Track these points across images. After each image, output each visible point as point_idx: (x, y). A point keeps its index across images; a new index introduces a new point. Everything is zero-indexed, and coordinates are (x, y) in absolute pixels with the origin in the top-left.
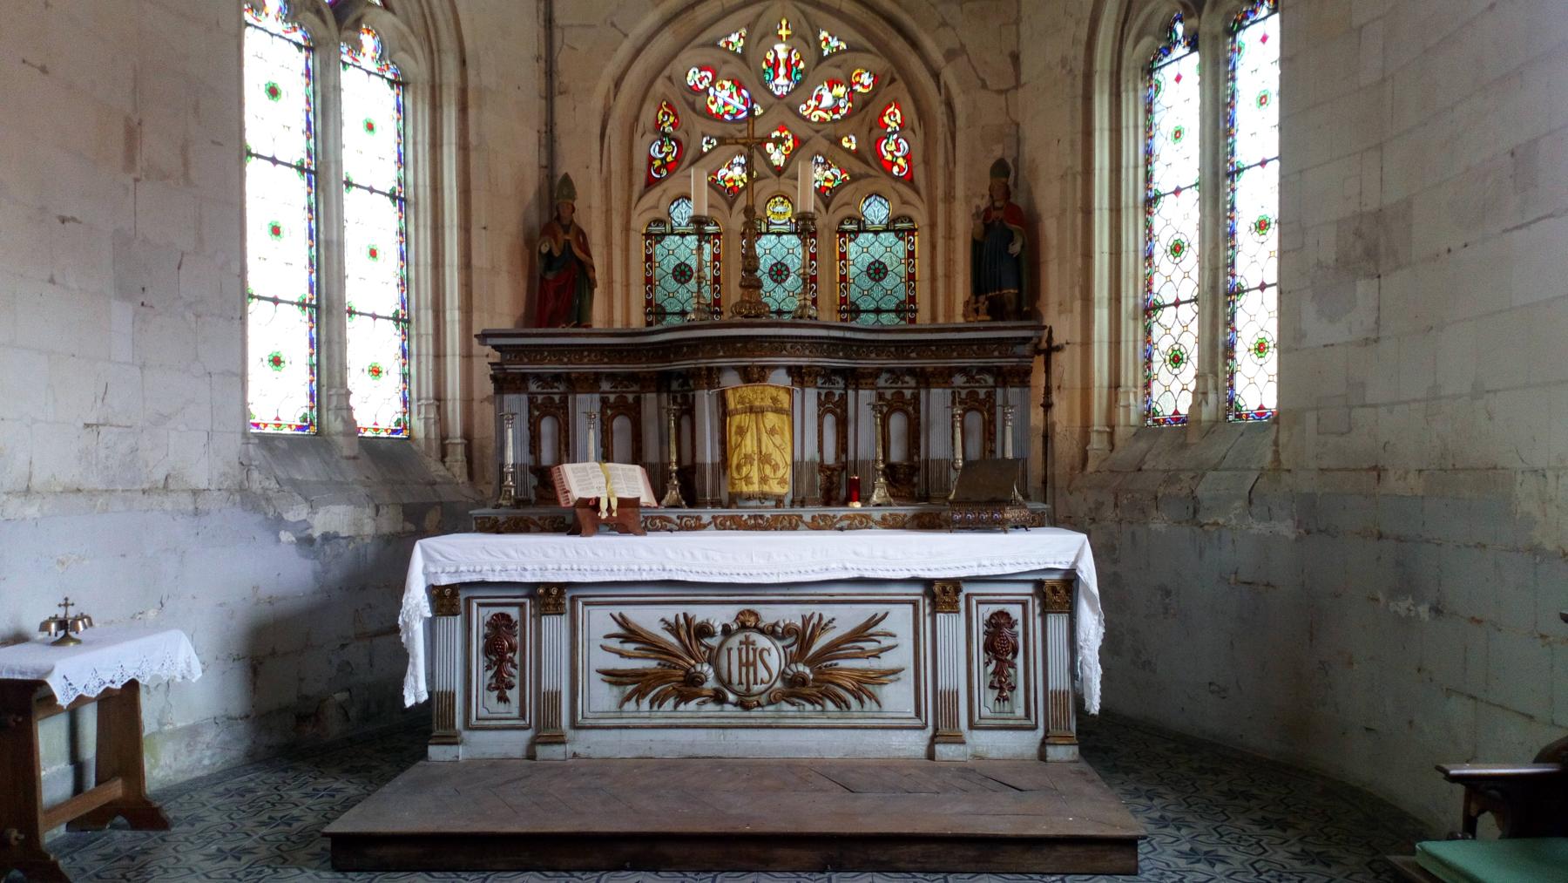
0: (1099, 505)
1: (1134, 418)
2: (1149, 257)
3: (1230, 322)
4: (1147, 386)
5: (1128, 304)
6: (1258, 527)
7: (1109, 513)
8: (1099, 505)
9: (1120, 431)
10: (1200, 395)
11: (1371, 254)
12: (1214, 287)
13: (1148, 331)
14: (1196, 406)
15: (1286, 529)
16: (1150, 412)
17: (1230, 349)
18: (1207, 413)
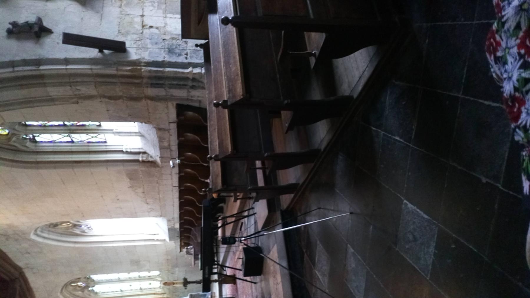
0: (176, 295)
1: (161, 290)
2: (131, 290)
3: (145, 277)
4: (155, 288)
5: (140, 293)
6: (177, 272)
7: (177, 294)
8: (176, 295)
9: (163, 292)
10: (157, 280)
11: (136, 262)
12: (138, 280)
13: (145, 289)
14: (159, 281)
15: (177, 269)
16: (160, 287)
17: (149, 276)
18: (160, 279)
